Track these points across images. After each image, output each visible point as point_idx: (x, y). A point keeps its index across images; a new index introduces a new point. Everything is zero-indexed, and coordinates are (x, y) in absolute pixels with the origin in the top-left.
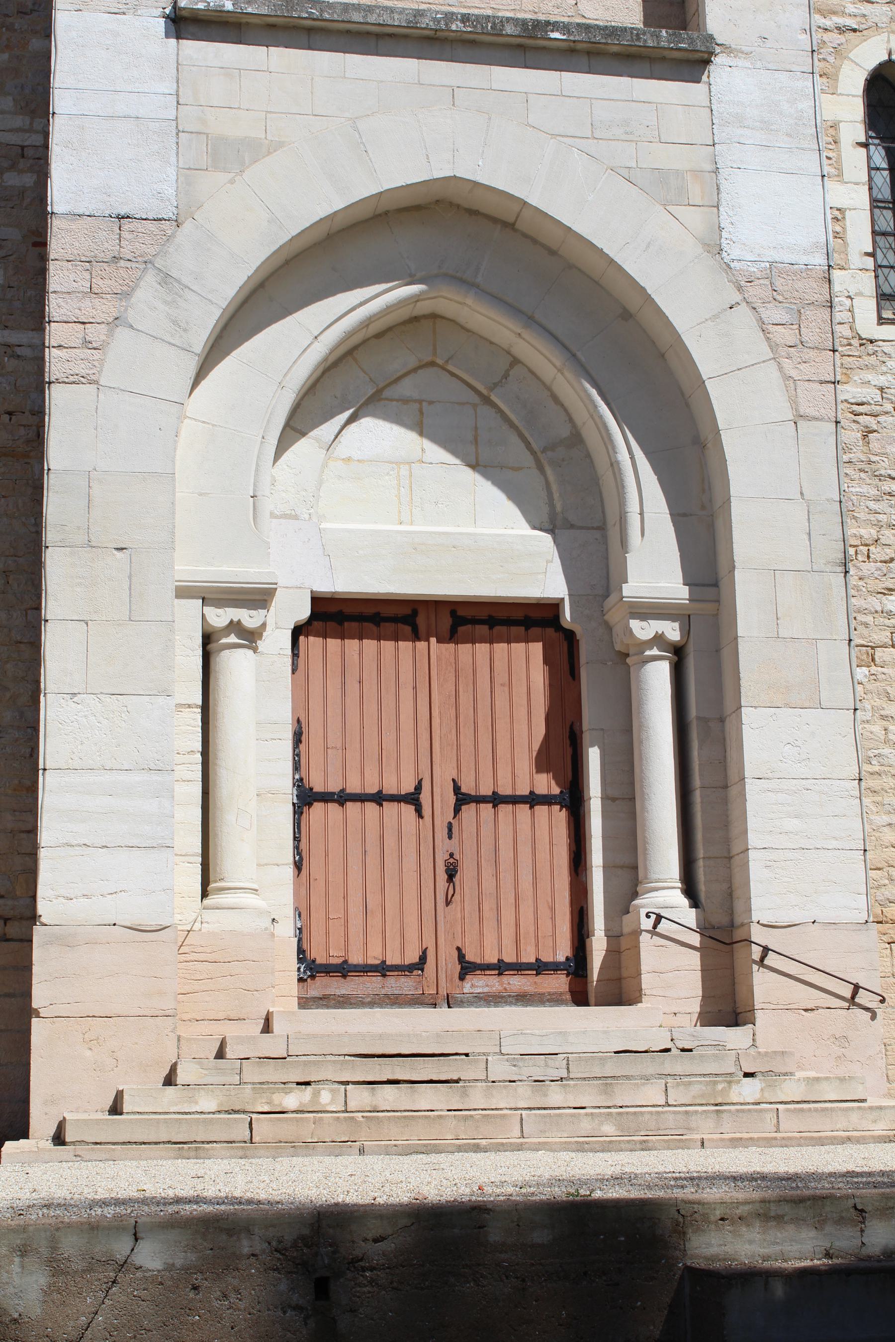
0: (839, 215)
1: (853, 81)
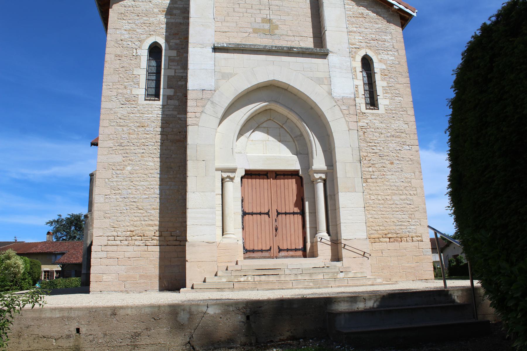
0: (357, 87)
1: (359, 59)
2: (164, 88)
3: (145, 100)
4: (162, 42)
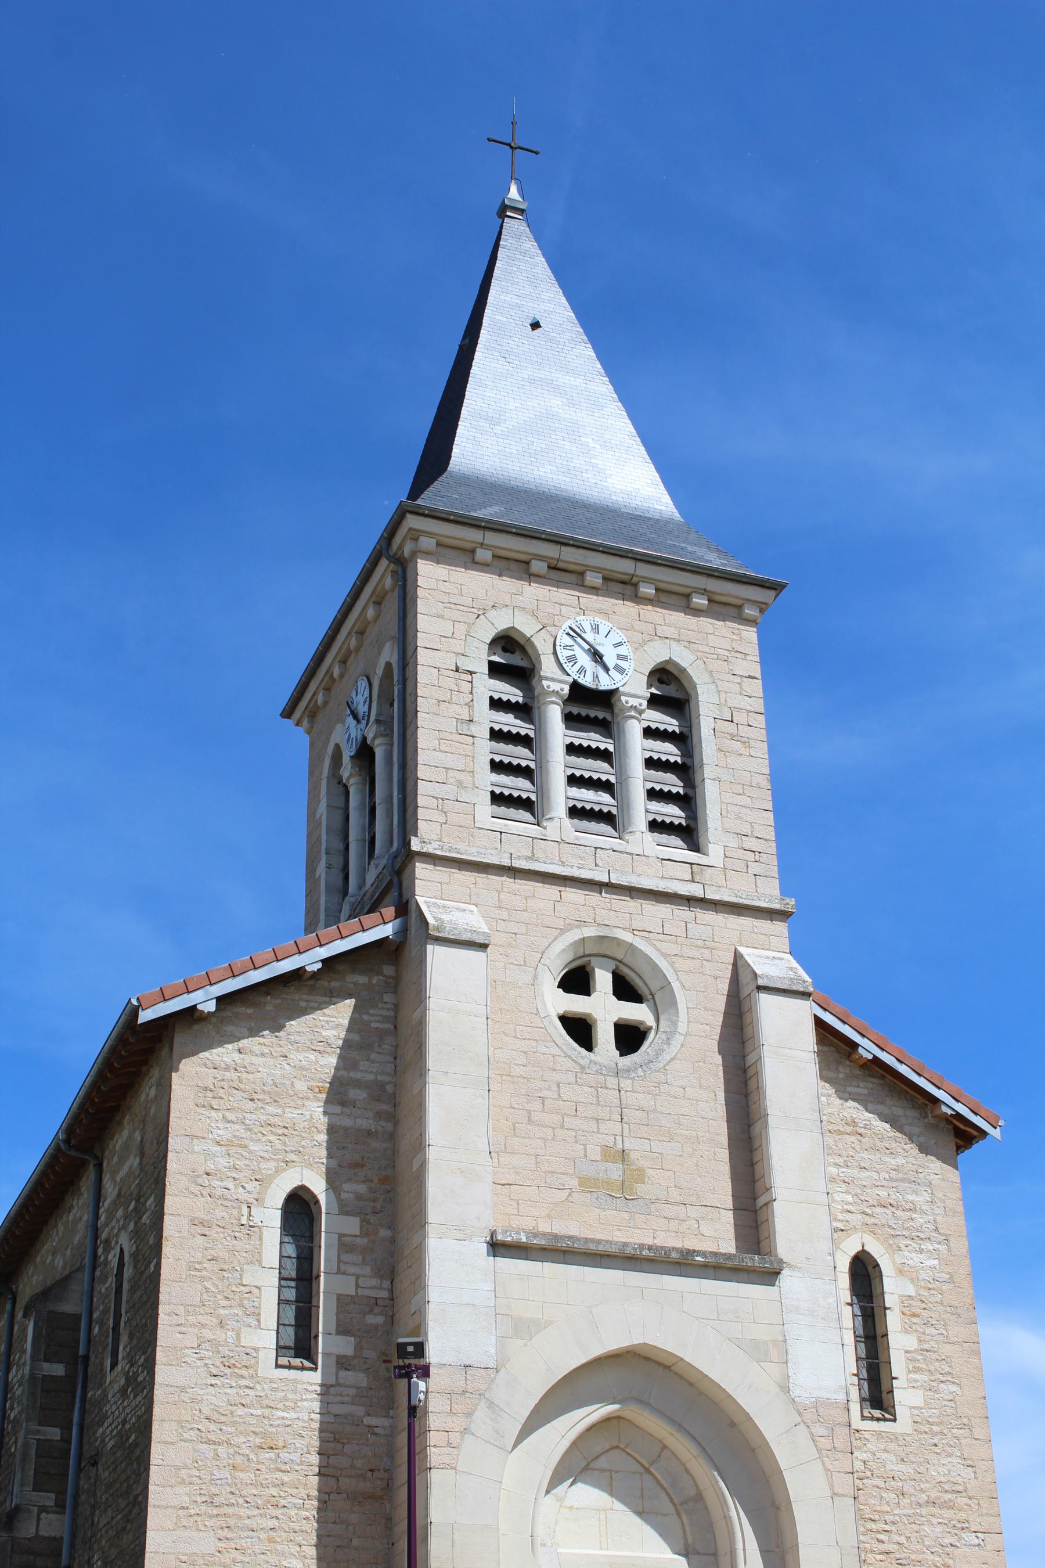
1: (844, 1265)
2: (327, 1334)
3: (278, 1366)
4: (318, 1186)
